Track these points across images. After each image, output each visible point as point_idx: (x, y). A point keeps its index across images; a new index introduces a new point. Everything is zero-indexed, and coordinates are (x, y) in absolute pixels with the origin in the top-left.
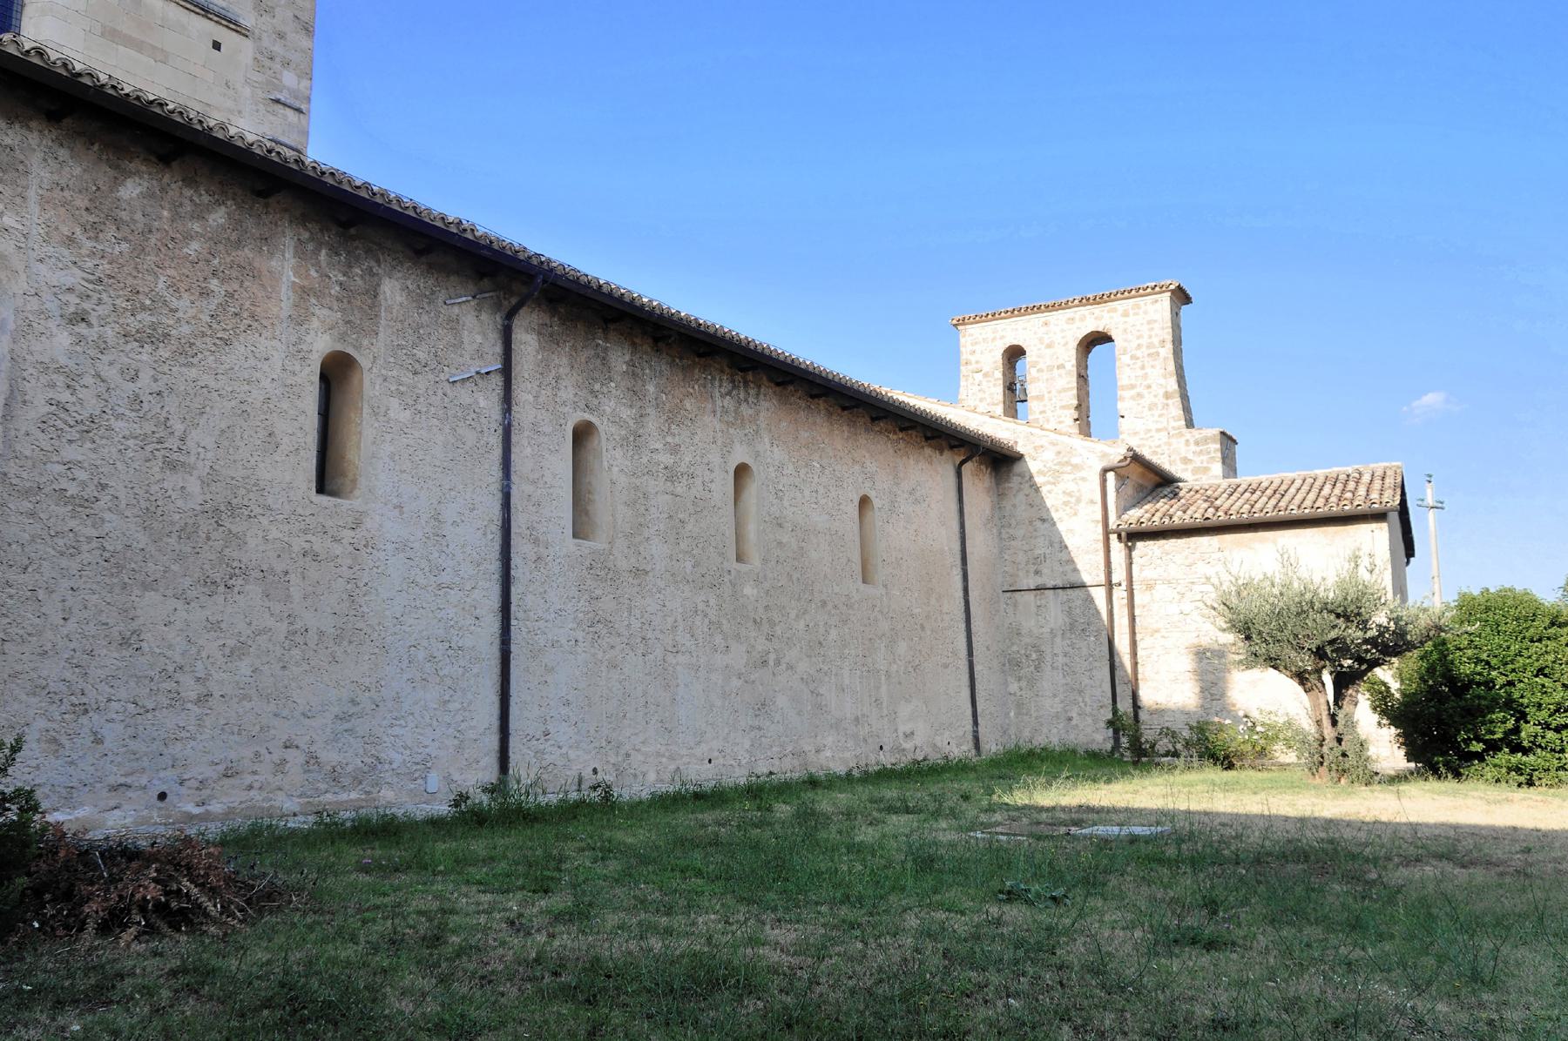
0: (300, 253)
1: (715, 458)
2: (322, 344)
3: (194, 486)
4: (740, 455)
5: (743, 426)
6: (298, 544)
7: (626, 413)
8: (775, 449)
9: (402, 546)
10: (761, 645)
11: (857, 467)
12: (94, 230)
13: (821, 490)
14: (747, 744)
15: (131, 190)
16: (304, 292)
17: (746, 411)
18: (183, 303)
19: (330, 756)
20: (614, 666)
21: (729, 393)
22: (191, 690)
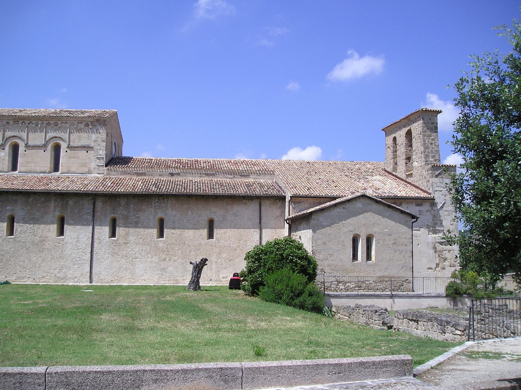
0: (55, 201)
1: (151, 217)
2: (58, 214)
3: (38, 238)
4: (160, 215)
5: (162, 208)
6: (53, 245)
7: (125, 213)
8: (173, 212)
9: (71, 243)
10: (164, 256)
11: (208, 211)
12: (26, 207)
13: (191, 219)
14: (157, 277)
15: (31, 199)
16: (55, 207)
17: (163, 205)
18: (37, 213)
19: (59, 275)
20: (117, 261)
21: (157, 202)
22: (38, 265)
